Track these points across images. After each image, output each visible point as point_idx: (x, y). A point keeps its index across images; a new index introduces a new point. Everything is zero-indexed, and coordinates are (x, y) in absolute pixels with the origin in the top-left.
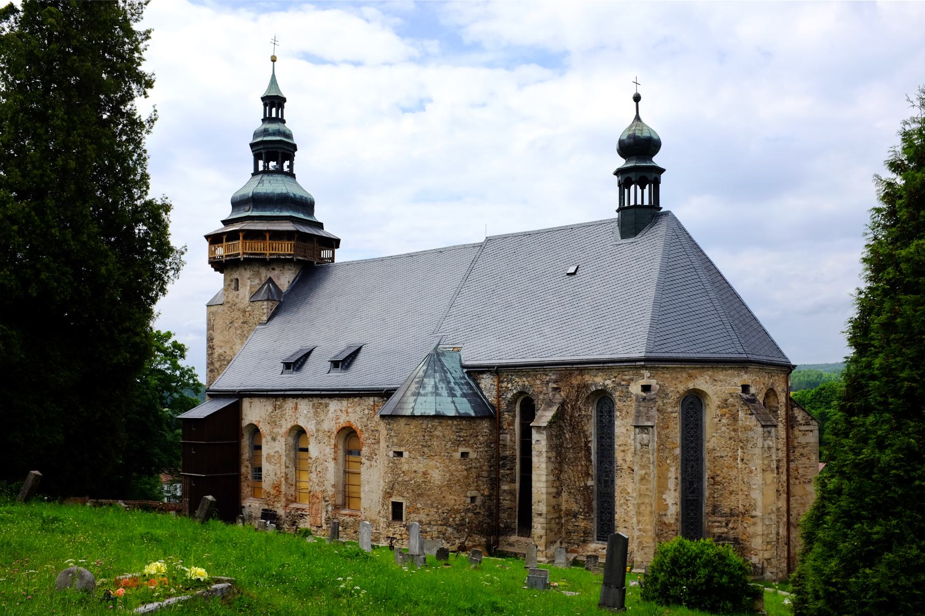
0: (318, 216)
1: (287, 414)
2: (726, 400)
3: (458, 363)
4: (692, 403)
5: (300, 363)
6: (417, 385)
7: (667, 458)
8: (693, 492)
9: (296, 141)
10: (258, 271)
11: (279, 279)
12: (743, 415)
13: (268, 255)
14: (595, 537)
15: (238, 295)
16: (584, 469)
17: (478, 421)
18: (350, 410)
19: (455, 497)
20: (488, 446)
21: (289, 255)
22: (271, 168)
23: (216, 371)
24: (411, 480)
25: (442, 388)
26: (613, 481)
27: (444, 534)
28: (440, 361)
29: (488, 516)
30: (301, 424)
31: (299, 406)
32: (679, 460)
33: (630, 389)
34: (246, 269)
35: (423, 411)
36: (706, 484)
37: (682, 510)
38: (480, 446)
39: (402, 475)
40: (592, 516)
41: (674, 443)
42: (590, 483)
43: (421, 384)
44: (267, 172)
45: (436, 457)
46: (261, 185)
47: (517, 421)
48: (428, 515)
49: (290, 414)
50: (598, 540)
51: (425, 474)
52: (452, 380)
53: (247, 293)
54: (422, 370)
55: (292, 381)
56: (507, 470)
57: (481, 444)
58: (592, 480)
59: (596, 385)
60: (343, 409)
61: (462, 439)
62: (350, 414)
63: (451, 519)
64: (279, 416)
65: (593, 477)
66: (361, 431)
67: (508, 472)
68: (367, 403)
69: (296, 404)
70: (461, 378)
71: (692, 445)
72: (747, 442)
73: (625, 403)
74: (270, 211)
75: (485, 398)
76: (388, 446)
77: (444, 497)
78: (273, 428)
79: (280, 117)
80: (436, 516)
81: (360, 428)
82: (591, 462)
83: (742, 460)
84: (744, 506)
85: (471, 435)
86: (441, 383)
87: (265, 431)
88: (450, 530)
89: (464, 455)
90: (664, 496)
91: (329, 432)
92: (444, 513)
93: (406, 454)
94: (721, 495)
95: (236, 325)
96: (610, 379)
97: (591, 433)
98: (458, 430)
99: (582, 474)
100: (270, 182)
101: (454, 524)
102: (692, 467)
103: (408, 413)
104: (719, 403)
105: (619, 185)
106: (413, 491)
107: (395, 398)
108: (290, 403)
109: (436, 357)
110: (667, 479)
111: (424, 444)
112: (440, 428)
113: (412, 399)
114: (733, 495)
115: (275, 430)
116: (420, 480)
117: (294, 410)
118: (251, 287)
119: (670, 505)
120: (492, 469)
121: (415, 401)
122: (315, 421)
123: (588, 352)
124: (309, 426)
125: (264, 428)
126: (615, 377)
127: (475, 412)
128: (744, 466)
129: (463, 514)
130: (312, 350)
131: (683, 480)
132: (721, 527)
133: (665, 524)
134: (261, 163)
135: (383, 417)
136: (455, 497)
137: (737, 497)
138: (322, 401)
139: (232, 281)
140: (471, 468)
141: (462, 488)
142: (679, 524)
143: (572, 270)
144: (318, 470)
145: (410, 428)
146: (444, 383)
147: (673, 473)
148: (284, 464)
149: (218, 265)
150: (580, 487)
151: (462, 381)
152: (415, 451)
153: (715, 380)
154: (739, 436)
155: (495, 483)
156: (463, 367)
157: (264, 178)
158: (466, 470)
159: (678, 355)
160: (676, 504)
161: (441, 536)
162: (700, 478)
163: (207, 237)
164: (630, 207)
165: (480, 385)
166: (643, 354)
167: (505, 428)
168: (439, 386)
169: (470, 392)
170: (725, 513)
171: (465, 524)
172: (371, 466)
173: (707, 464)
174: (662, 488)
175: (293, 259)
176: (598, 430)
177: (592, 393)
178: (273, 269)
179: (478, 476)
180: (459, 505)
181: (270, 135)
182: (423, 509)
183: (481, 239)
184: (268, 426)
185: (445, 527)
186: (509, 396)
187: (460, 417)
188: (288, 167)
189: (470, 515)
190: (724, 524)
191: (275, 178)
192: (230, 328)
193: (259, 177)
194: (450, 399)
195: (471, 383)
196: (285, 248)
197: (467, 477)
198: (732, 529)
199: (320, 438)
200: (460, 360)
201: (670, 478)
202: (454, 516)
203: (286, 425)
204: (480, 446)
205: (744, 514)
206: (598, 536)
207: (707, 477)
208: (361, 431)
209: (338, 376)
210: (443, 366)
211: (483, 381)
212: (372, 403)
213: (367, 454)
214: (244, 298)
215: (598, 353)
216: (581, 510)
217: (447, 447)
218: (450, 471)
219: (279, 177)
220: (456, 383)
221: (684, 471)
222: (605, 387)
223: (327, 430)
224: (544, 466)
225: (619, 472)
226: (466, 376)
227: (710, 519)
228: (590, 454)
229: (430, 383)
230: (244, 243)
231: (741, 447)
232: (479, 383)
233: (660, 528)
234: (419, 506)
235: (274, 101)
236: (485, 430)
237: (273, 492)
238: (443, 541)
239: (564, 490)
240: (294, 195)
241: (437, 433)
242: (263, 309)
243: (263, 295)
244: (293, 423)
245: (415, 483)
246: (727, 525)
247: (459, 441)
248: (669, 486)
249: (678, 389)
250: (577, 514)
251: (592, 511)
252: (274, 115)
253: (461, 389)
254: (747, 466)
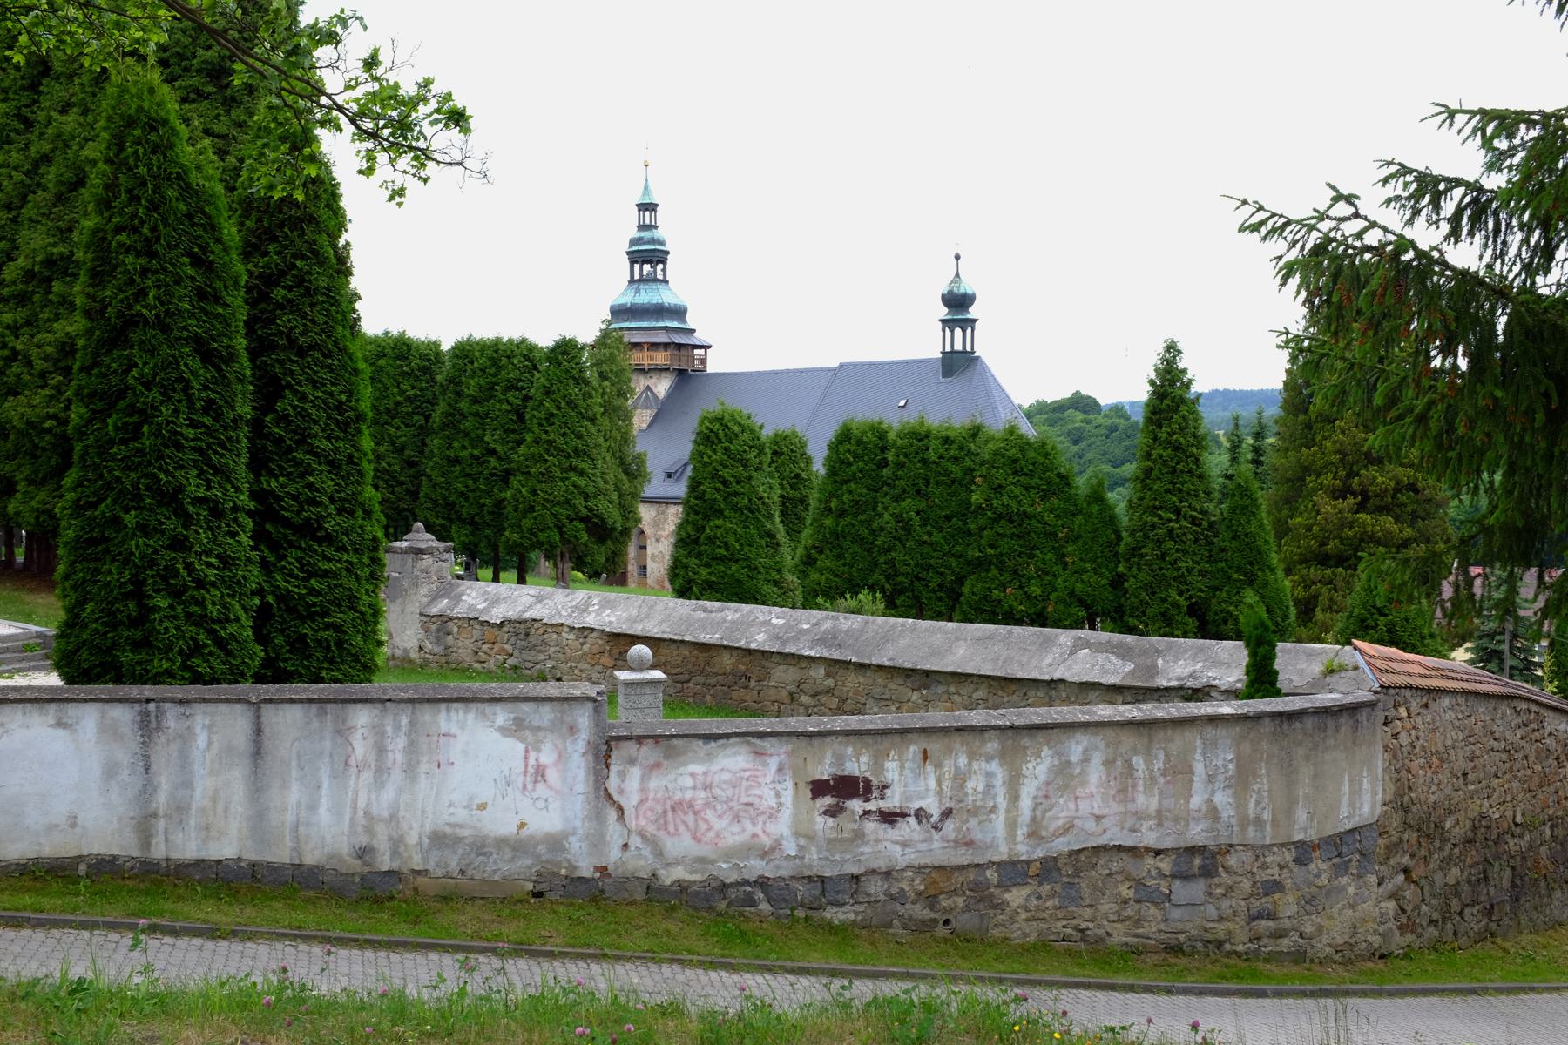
0: (691, 324)
44: (642, 280)
134: (637, 266)
143: (902, 403)
164: (953, 352)
181: (645, 243)
183: (837, 365)
193: (635, 286)
196: (662, 358)
219: (653, 286)
235: (648, 207)
252: (648, 222)
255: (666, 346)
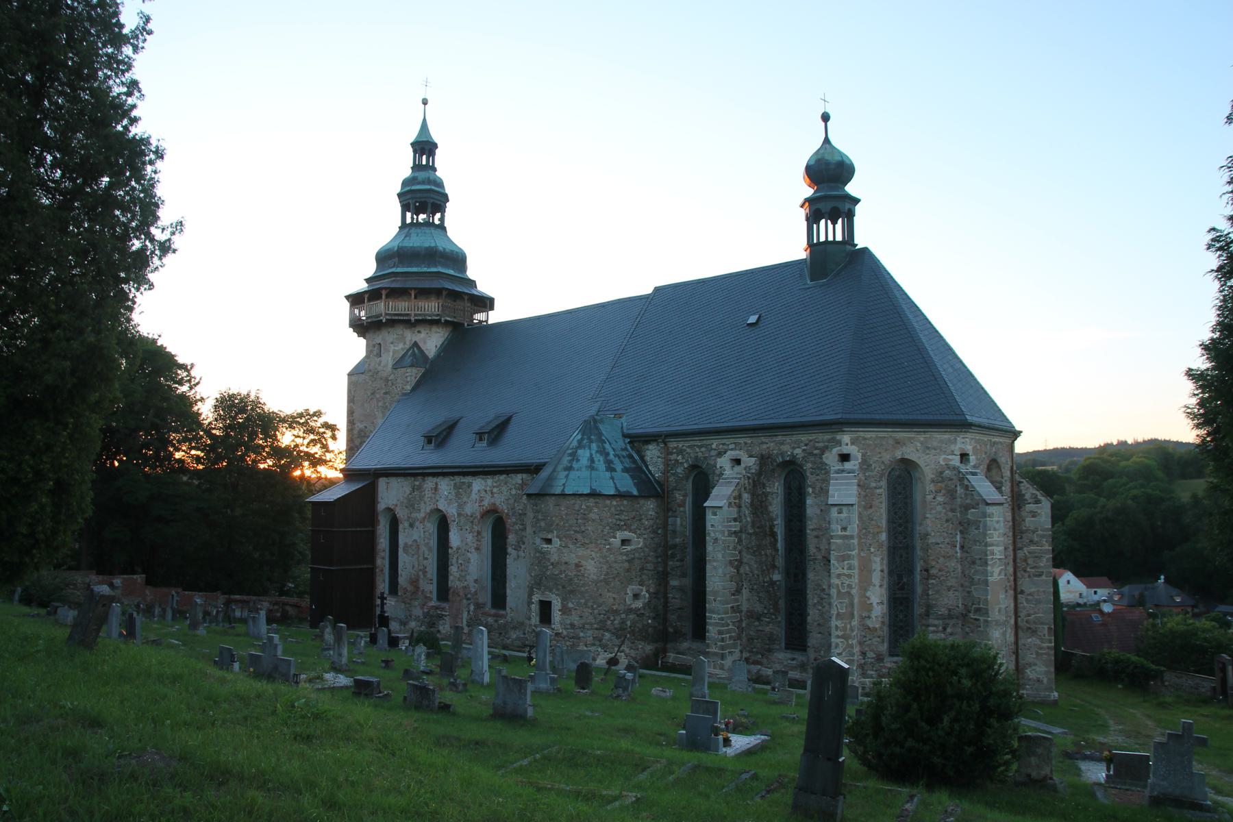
0: (471, 274)
1: (427, 496)
2: (941, 473)
3: (619, 431)
4: (899, 477)
5: (442, 436)
6: (570, 458)
7: (870, 545)
8: (902, 588)
9: (447, 192)
10: (402, 335)
11: (425, 343)
12: (962, 491)
13: (413, 315)
14: (783, 645)
15: (380, 362)
16: (770, 559)
17: (642, 501)
18: (495, 490)
19: (614, 596)
20: (655, 532)
21: (438, 315)
22: (420, 220)
24: (561, 574)
25: (599, 460)
26: (804, 575)
27: (600, 641)
28: (597, 429)
29: (654, 618)
30: (441, 507)
31: (439, 487)
32: (885, 548)
33: (824, 460)
34: (389, 332)
35: (576, 489)
36: (918, 578)
37: (890, 610)
38: (644, 532)
39: (551, 567)
40: (779, 619)
41: (879, 527)
42: (776, 577)
43: (574, 455)
45: (590, 546)
46: (408, 238)
47: (689, 500)
48: (581, 617)
49: (429, 496)
50: (786, 648)
51: (578, 565)
52: (612, 453)
53: (390, 359)
54: (576, 439)
55: (432, 458)
56: (677, 561)
57: (645, 529)
58: (779, 573)
59: (782, 454)
60: (488, 489)
61: (623, 523)
62: (495, 495)
63: (609, 622)
64: (418, 499)
65: (780, 570)
66: (507, 514)
67: (678, 564)
68: (514, 482)
69: (436, 484)
70: (622, 450)
71: (900, 529)
72: (969, 524)
73: (818, 477)
74: (417, 266)
75: (651, 474)
76: (534, 532)
77: (601, 595)
78: (411, 513)
79: (431, 164)
80: (591, 617)
81: (506, 511)
82: (778, 550)
83: (962, 547)
84: (965, 605)
85: (634, 518)
86: (598, 455)
87: (402, 517)
88: (607, 635)
89: (624, 542)
90: (868, 594)
91: (472, 516)
92: (600, 614)
93: (557, 542)
94: (937, 592)
95: (378, 396)
96: (799, 447)
97: (777, 515)
98: (617, 513)
99: (766, 566)
100: (417, 236)
101: (612, 628)
102: (901, 557)
103: (558, 491)
104: (934, 476)
105: (807, 219)
106: (564, 587)
107: (544, 474)
108: (430, 483)
109: (592, 423)
110: (870, 571)
111: (578, 529)
112: (596, 510)
113: (563, 474)
114: (951, 592)
115: (414, 515)
116: (572, 574)
117: (433, 491)
118: (394, 352)
119: (875, 604)
120: (659, 560)
121: (567, 476)
122: (456, 504)
123: (773, 416)
124: (451, 511)
125: (401, 513)
126: (806, 445)
127: (638, 490)
128: (965, 554)
129: (623, 616)
130: (458, 421)
131: (891, 573)
132: (937, 632)
133: (869, 628)
134: (409, 215)
135: (529, 496)
136: (614, 596)
137: (957, 593)
138: (464, 481)
139: (374, 346)
140: (633, 559)
141: (622, 583)
142: (886, 629)
143: (753, 319)
144: (460, 562)
145: (560, 510)
146: (601, 455)
147: (878, 564)
148: (421, 555)
149: (360, 327)
150: (764, 582)
151: (624, 453)
152: (566, 538)
153: (928, 448)
154: (957, 518)
155: (663, 577)
156: (625, 436)
157: (410, 231)
158: (628, 561)
159: (882, 417)
160: (882, 603)
161: (597, 643)
162: (911, 572)
163: (348, 297)
164: (819, 243)
165: (645, 458)
166: (839, 416)
167: (674, 510)
168: (595, 459)
169: (633, 466)
170: (942, 615)
171: (626, 629)
172: (518, 556)
173: (919, 553)
174: (865, 583)
175: (440, 320)
176: (785, 511)
177: (778, 465)
178: (419, 332)
179: (642, 569)
180: (619, 605)
181: (419, 183)
182: (576, 609)
184: (406, 510)
185: (601, 631)
186: (679, 470)
187: (620, 496)
188: (439, 220)
189: (632, 616)
190: (941, 628)
191: (423, 231)
192: (371, 399)
194: (608, 474)
195: (636, 457)
196: (431, 307)
197: (628, 570)
198: (951, 634)
199: (461, 524)
200: (622, 428)
201: (875, 570)
202: (612, 618)
203: (426, 508)
204: (644, 532)
205: (964, 616)
206: (786, 644)
207: (919, 569)
208: (507, 514)
209: (485, 450)
210: (600, 434)
211: (648, 453)
212: (520, 482)
213: (514, 543)
214: (386, 366)
215: (785, 416)
216: (766, 612)
217: (605, 533)
218: (607, 562)
219: (427, 230)
220: (615, 455)
221: (892, 561)
222: (794, 457)
223: (469, 514)
224: (720, 556)
225: (812, 563)
226: (629, 447)
227: (924, 622)
228: (776, 540)
229: (584, 454)
230: (387, 303)
231: (961, 532)
232: (645, 456)
233: (863, 633)
234: (570, 605)
235: (424, 147)
236: (650, 513)
237: (410, 588)
238: (600, 649)
239: (745, 586)
240: (444, 249)
241: (592, 516)
242: (406, 377)
243: (408, 360)
244: (433, 507)
245: (566, 576)
246: (945, 629)
247: (618, 525)
248: (873, 581)
249: (883, 459)
250: (760, 615)
251: (779, 612)
252: (424, 162)
253: (622, 462)
254: (968, 555)
255: (438, 292)
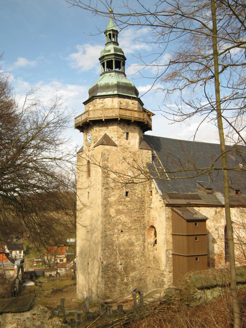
23: (111, 189)
34: (135, 129)
87: (210, 225)
